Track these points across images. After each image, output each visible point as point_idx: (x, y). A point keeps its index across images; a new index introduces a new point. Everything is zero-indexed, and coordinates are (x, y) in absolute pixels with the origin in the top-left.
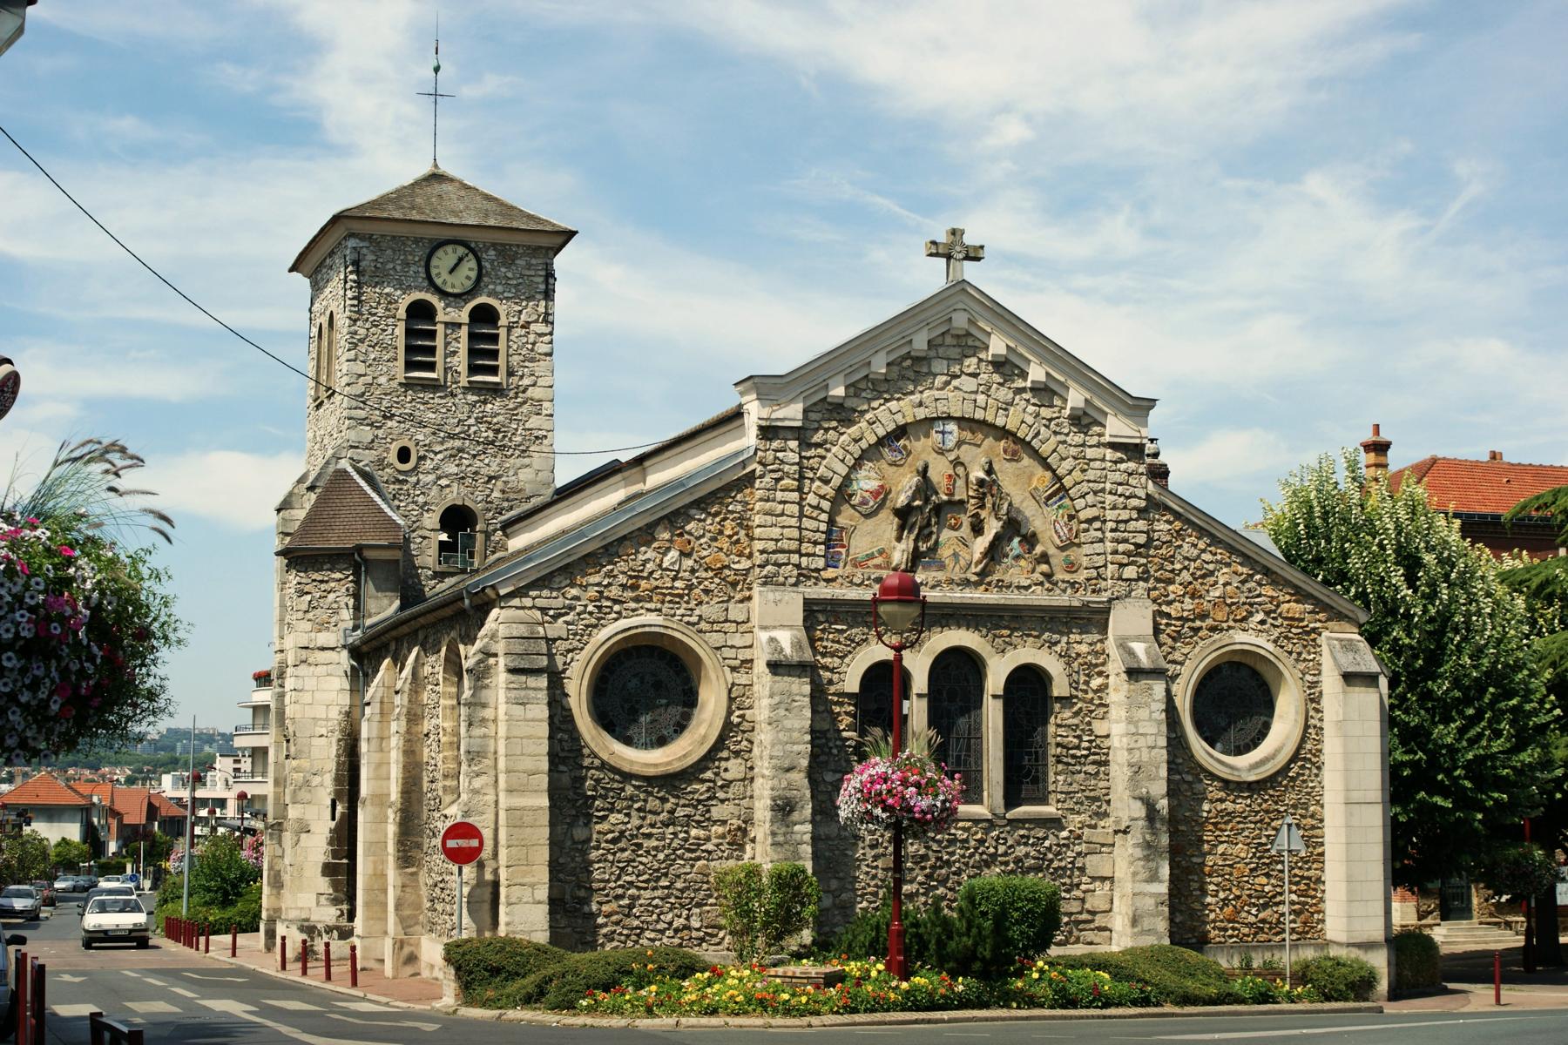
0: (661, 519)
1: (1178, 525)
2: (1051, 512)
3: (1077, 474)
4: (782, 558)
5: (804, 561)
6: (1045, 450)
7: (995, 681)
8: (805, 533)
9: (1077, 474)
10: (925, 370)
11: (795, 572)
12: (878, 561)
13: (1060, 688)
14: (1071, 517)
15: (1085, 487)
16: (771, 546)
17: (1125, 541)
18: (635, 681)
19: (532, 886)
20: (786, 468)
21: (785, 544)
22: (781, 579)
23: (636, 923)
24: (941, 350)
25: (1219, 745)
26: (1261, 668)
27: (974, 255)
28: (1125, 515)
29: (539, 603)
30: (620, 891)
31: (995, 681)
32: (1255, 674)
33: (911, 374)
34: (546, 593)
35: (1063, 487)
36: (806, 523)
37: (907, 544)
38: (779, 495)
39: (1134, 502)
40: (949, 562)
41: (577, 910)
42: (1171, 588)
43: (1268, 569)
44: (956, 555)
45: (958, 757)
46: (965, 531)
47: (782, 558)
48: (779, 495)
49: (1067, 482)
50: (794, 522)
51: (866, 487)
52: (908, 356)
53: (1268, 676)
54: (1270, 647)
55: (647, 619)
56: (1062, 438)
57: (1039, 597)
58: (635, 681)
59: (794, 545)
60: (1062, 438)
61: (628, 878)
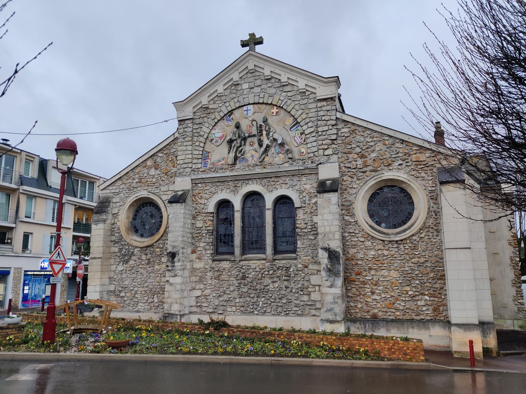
0: (149, 158)
1: (353, 128)
2: (292, 133)
3: (304, 116)
4: (185, 166)
5: (194, 166)
6: (289, 110)
7: (269, 203)
8: (194, 156)
9: (304, 116)
10: (240, 89)
11: (190, 170)
12: (223, 162)
13: (297, 204)
14: (302, 134)
15: (307, 120)
16: (182, 162)
17: (327, 139)
18: (145, 215)
19: (95, 286)
20: (188, 134)
21: (186, 161)
22: (185, 173)
23: (136, 300)
24: (246, 80)
25: (383, 225)
26: (403, 186)
27: (260, 42)
28: (326, 128)
29: (112, 191)
30: (132, 288)
31: (269, 203)
32: (403, 190)
33: (234, 91)
34: (114, 188)
35: (297, 123)
36: (195, 152)
37: (232, 155)
38: (185, 144)
39: (329, 123)
40: (250, 159)
41: (119, 295)
42: (350, 156)
43: (403, 140)
44: (252, 156)
45: (258, 235)
46: (256, 145)
47: (185, 166)
48: (185, 144)
49: (299, 120)
50: (190, 152)
51: (217, 136)
52: (232, 85)
53: (409, 190)
54: (405, 176)
55: (143, 194)
56: (297, 103)
57: (287, 167)
58: (145, 215)
59: (190, 161)
60: (297, 103)
61: (134, 284)
